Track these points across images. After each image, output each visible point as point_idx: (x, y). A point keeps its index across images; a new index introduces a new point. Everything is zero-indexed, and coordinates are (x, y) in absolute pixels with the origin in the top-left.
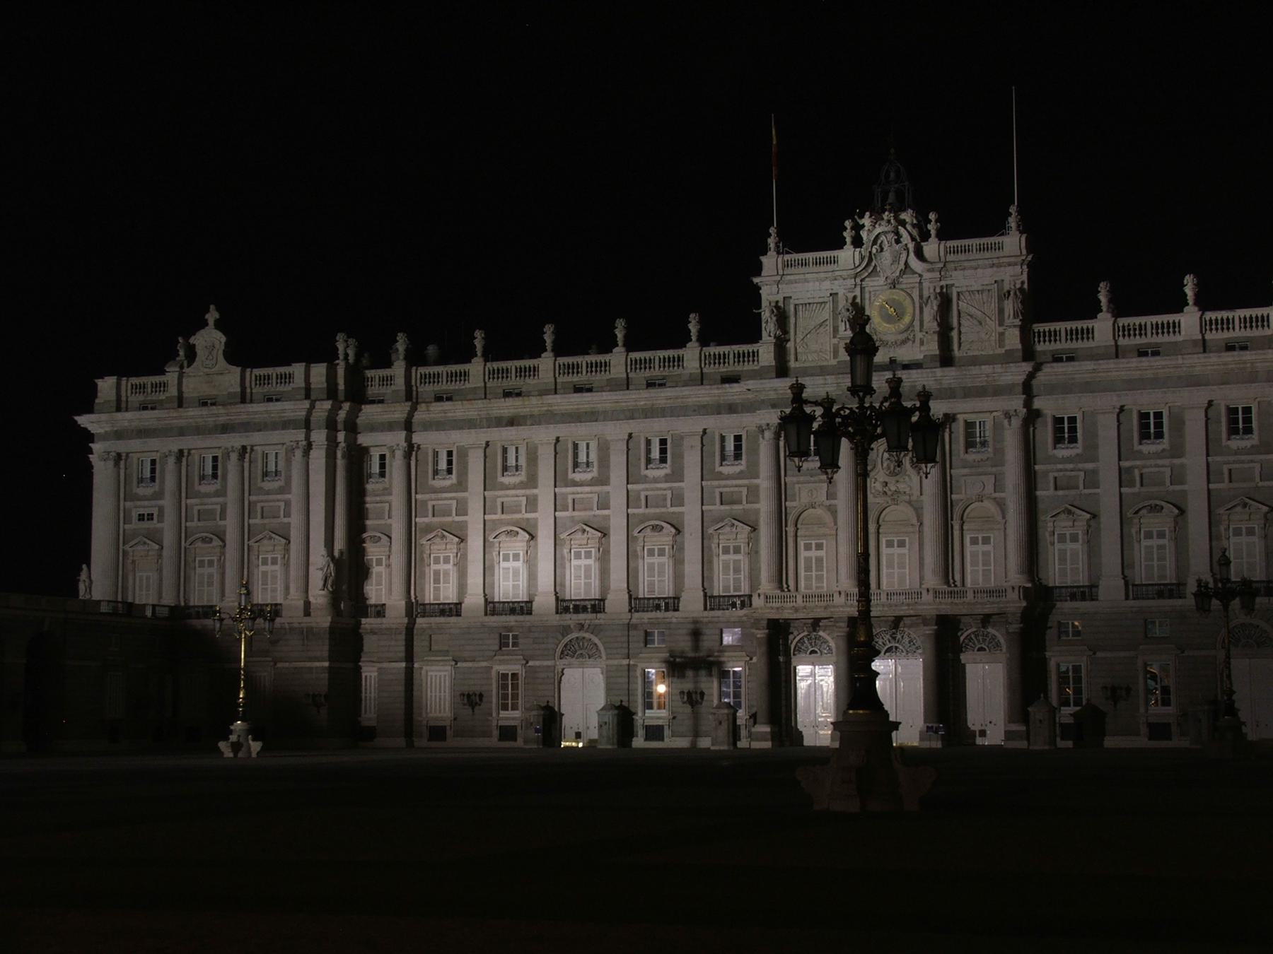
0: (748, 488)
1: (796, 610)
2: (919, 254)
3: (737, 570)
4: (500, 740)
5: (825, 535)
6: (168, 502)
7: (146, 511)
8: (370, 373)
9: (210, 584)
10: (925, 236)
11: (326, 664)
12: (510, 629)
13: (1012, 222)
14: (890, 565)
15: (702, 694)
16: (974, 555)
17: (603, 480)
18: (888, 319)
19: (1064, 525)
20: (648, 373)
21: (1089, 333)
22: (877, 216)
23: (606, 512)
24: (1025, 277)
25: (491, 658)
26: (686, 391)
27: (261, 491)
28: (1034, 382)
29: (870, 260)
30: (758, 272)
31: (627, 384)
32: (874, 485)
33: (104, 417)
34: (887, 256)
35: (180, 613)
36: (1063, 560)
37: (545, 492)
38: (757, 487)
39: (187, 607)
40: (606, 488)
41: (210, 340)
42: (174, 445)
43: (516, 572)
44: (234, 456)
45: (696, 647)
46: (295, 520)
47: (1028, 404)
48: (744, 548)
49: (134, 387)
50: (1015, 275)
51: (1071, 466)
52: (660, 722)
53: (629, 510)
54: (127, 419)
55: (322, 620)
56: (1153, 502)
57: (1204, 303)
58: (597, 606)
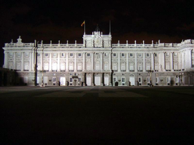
1: (88, 72)
3: (80, 68)
9: (19, 67)
10: (101, 34)
13: (110, 34)
15: (76, 80)
16: (105, 67)
17: (65, 57)
19: (115, 64)
20: (71, 46)
21: (126, 45)
22: (96, 31)
25: (52, 76)
26: (75, 48)
27: (26, 57)
30: (83, 37)
31: (68, 47)
32: (95, 59)
33: (7, 48)
35: (16, 70)
36: (114, 68)
37: (59, 58)
39: (17, 70)
40: (66, 58)
42: (15, 51)
50: (110, 39)
54: (10, 48)
57: (137, 43)
58: (65, 71)
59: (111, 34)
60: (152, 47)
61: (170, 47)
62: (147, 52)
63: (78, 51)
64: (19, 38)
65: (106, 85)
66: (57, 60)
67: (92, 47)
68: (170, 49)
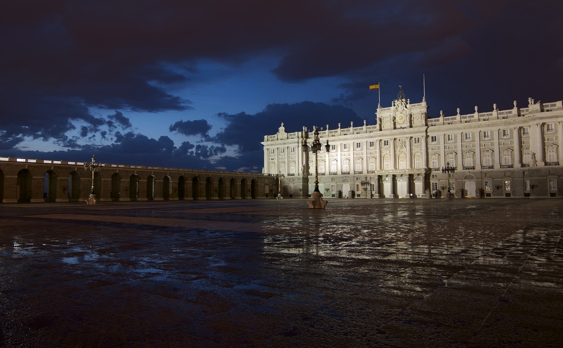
0: (375, 151)
2: (406, 107)
4: (332, 197)
5: (389, 160)
6: (276, 157)
7: (272, 158)
8: (309, 133)
9: (283, 170)
10: (407, 103)
11: (302, 184)
12: (333, 177)
13: (424, 100)
14: (401, 165)
15: (367, 189)
16: (417, 163)
18: (400, 119)
19: (433, 157)
22: (398, 100)
23: (350, 156)
24: (426, 110)
25: (330, 182)
26: (363, 134)
28: (428, 130)
29: (397, 108)
32: (398, 151)
34: (400, 107)
36: (433, 163)
38: (376, 151)
40: (349, 152)
41: (282, 129)
42: (277, 147)
43: (334, 167)
44: (286, 148)
45: (366, 180)
46: (297, 159)
47: (426, 134)
48: (374, 162)
49: (270, 137)
50: (424, 110)
51: (435, 146)
52: (360, 194)
53: (342, 157)
54: (269, 143)
55: (301, 176)
56: (451, 152)
59: (426, 101)
60: (514, 116)
61: (557, 109)
62: (502, 128)
63: (369, 137)
64: (281, 126)
65: (418, 197)
66: (337, 155)
67: (390, 130)
68: (555, 114)
